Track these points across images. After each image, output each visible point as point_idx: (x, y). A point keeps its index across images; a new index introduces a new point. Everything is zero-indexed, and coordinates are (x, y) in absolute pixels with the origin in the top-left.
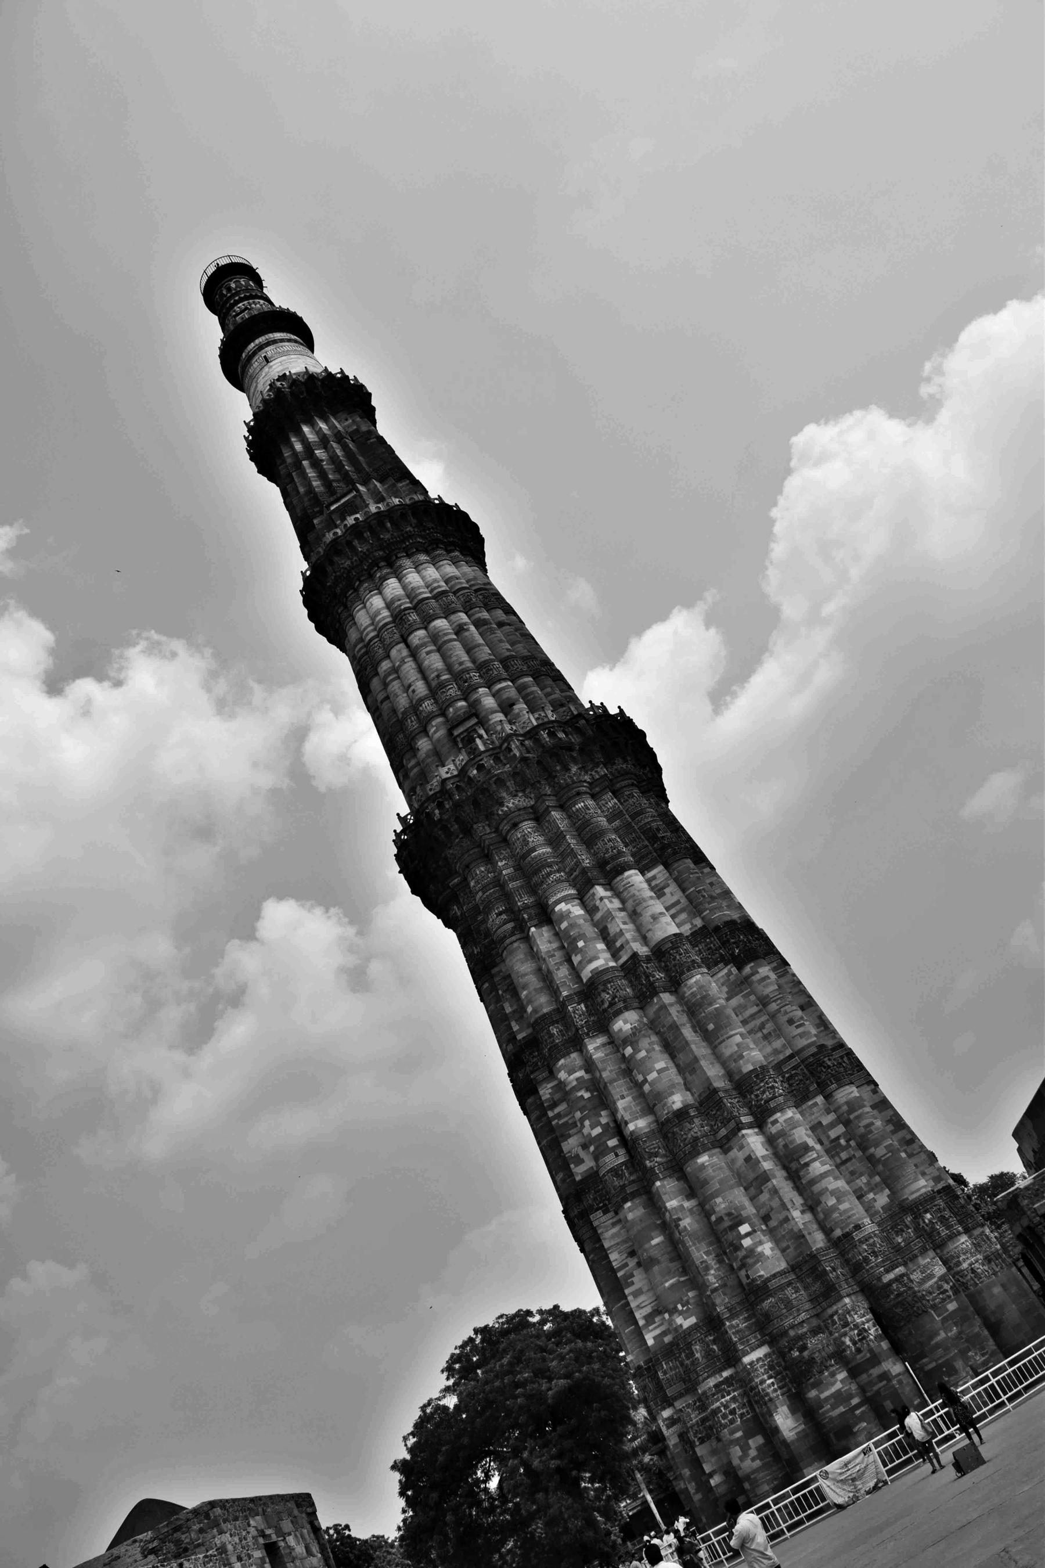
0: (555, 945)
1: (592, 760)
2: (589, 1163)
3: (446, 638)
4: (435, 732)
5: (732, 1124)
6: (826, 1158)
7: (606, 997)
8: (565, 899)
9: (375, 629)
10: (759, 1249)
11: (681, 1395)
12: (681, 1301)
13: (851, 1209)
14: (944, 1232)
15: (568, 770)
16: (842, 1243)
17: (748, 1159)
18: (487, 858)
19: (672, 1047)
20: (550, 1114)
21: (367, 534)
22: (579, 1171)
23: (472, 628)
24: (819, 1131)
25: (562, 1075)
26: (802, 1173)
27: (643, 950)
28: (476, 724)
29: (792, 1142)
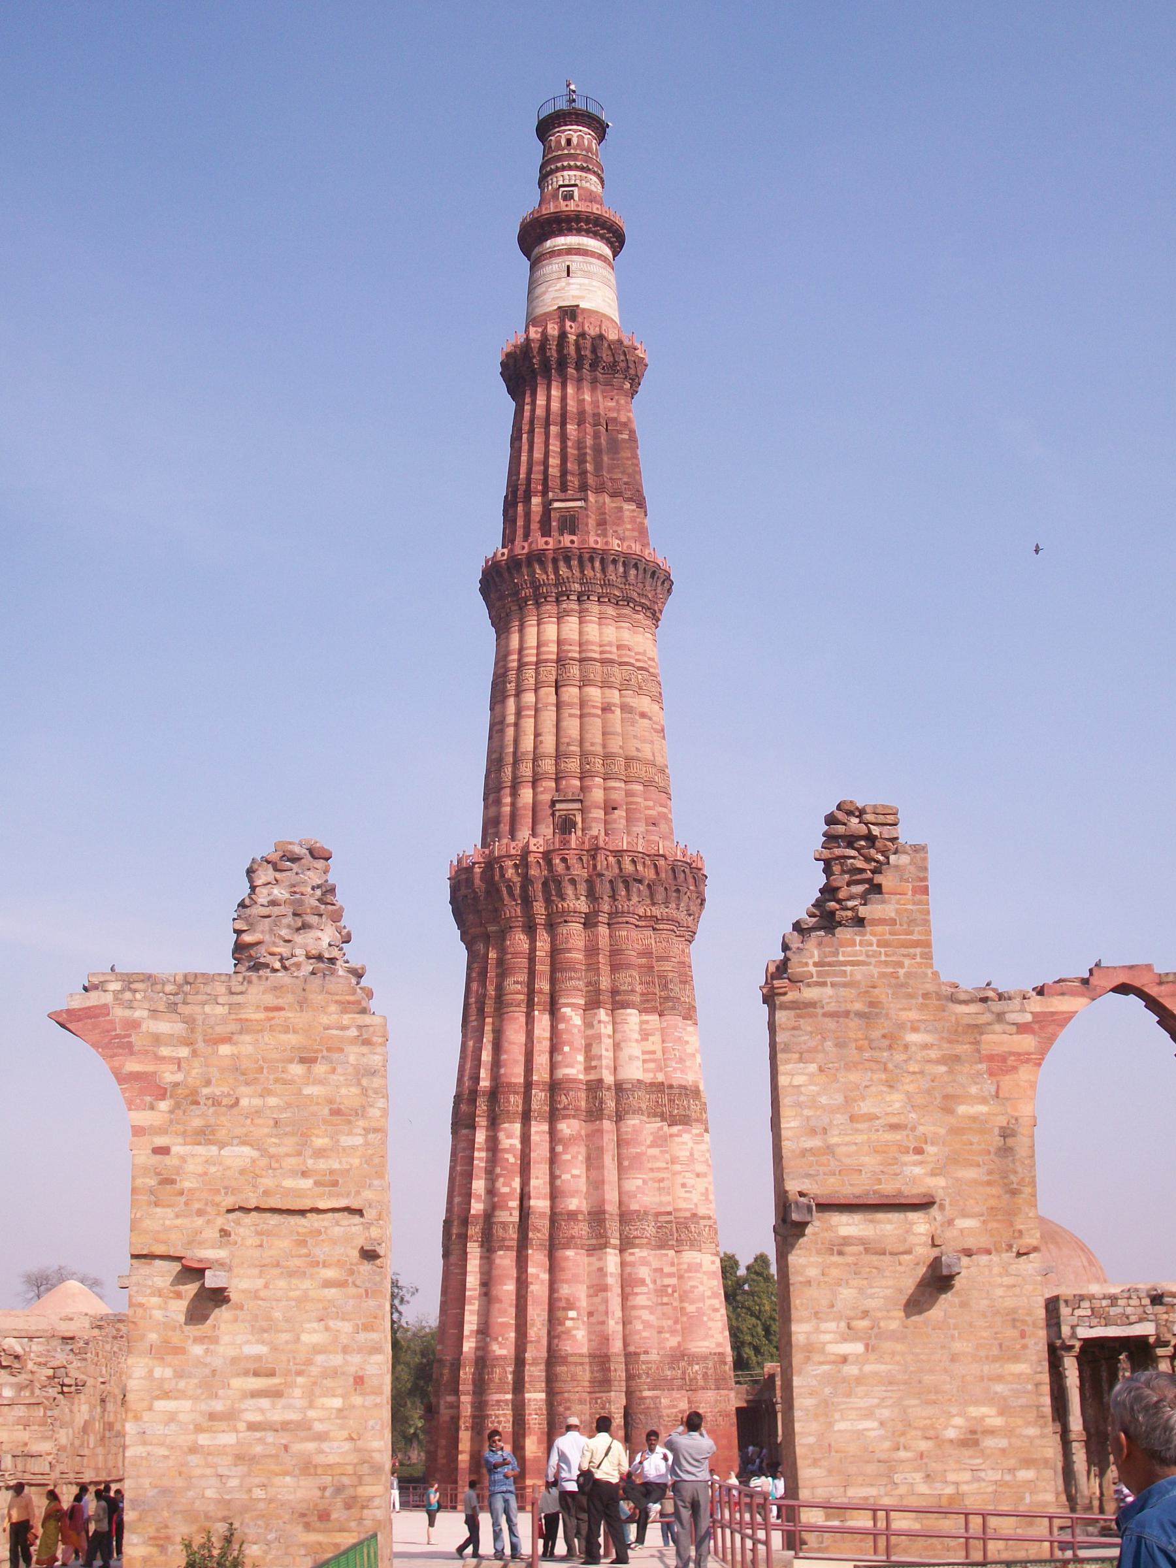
0: (548, 1035)
1: (652, 899)
4: (542, 793)
5: (602, 1241)
10: (574, 1332)
14: (701, 1383)
15: (630, 900)
16: (630, 1357)
17: (600, 1270)
18: (530, 930)
19: (593, 1161)
20: (476, 1154)
21: (575, 563)
24: (658, 1274)
25: (501, 1135)
26: (630, 1298)
27: (609, 1079)
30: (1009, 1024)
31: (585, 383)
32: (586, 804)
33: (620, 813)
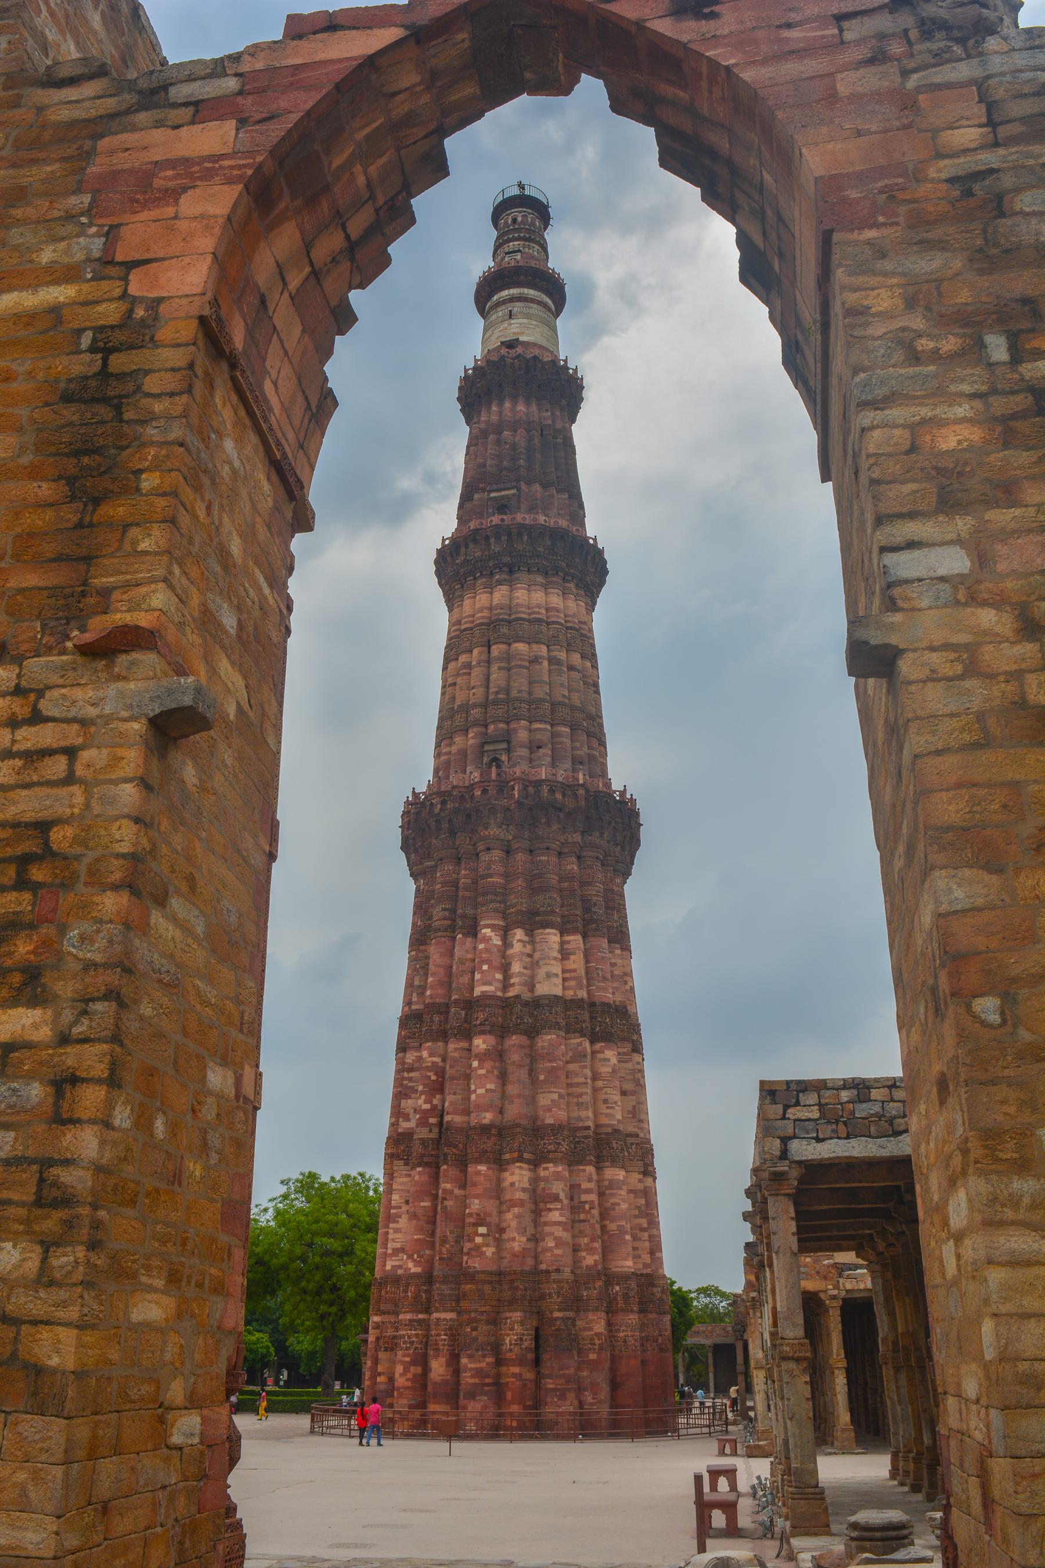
0: (470, 956)
2: (411, 1124)
3: (520, 663)
6: (567, 1213)
7: (482, 1016)
8: (493, 927)
9: (473, 622)
11: (388, 1313)
12: (418, 1253)
13: (562, 1256)
14: (621, 1304)
21: (504, 538)
22: (404, 1125)
23: (546, 663)
25: (425, 1054)
27: (527, 996)
28: (504, 749)
29: (549, 1189)
30: (174, 106)
31: (521, 400)
32: (513, 743)
33: (546, 751)
